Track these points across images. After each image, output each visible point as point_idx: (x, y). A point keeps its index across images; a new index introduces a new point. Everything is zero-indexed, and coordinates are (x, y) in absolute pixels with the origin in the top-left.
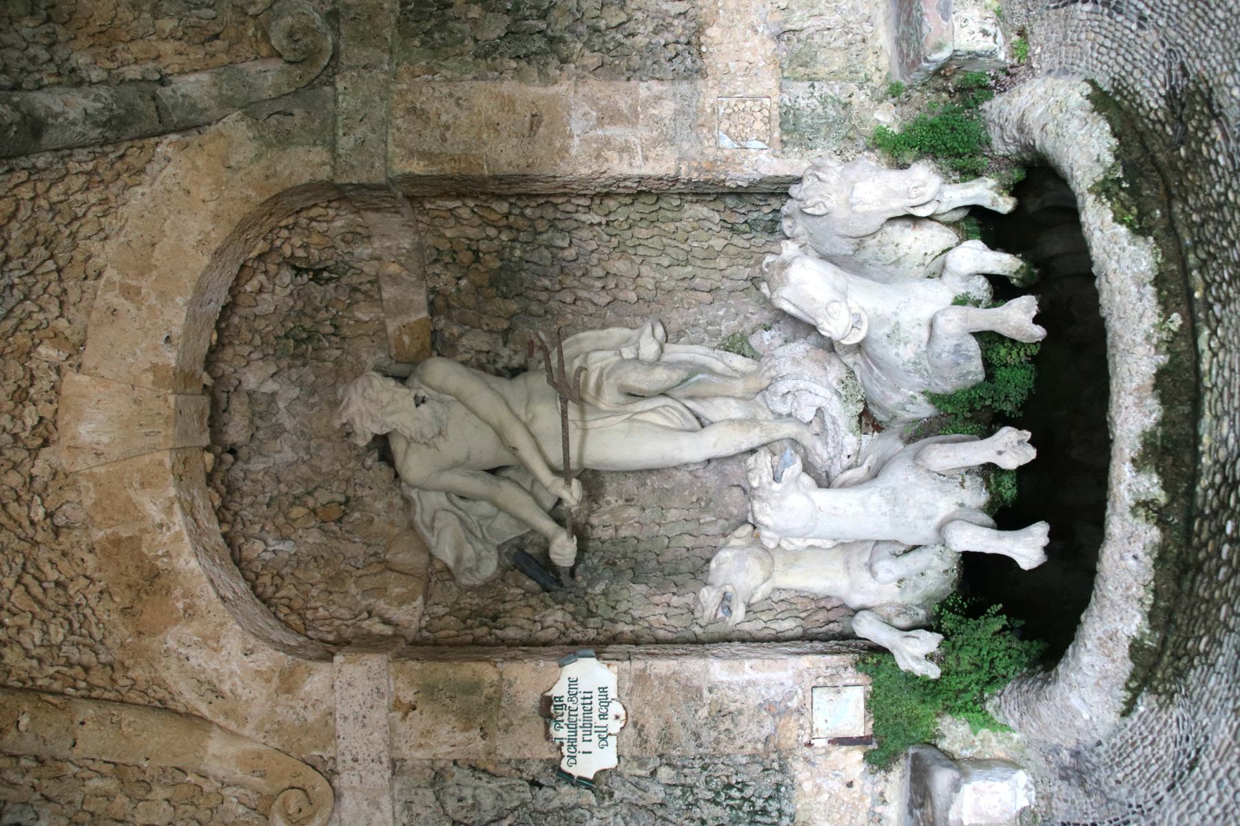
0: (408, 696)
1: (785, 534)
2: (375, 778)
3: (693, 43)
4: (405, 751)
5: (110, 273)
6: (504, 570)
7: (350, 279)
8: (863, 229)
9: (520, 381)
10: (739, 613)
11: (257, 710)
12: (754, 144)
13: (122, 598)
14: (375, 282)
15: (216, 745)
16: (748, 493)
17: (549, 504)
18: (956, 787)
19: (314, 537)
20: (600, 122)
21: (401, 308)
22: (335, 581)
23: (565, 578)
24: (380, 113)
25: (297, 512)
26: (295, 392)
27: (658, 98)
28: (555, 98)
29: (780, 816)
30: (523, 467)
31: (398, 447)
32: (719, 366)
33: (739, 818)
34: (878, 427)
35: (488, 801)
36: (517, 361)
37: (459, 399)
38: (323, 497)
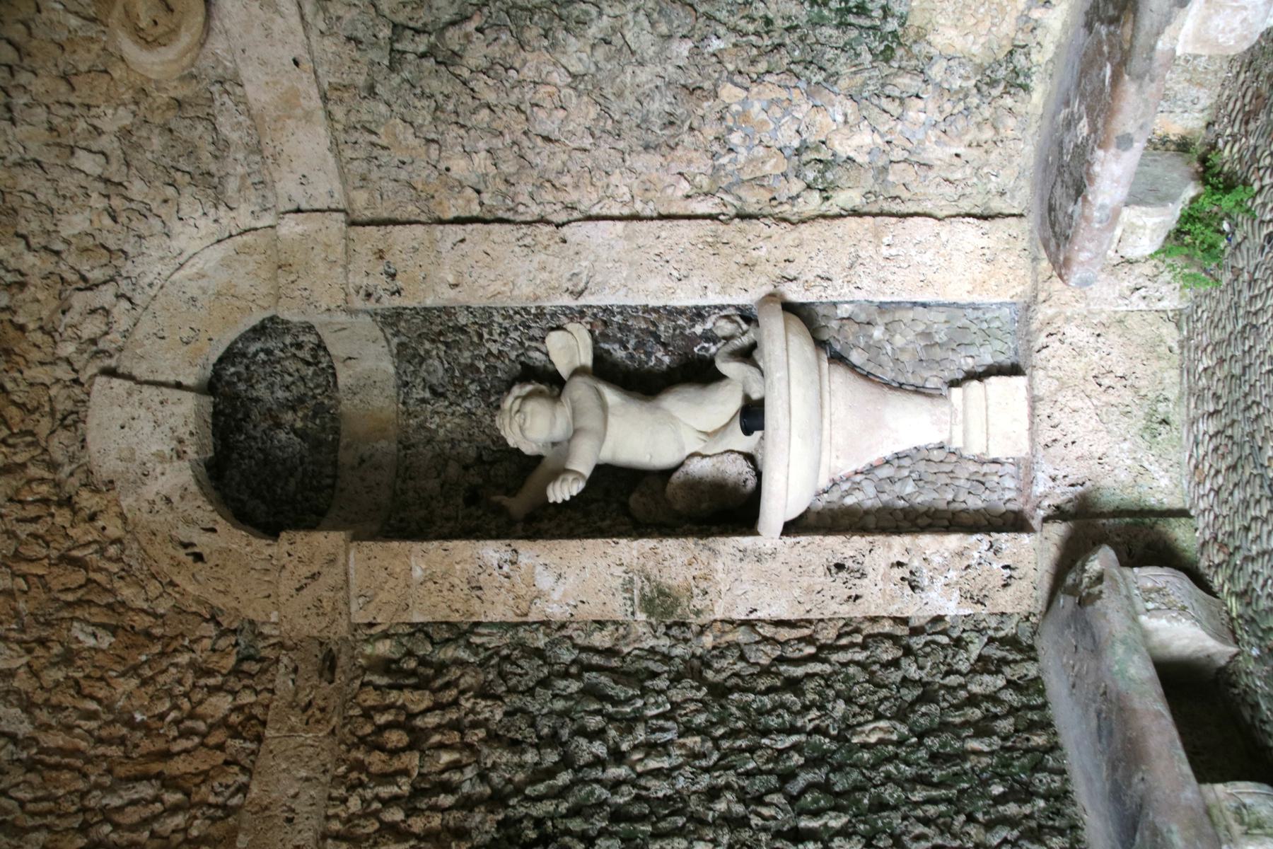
29: (885, 17)
33: (823, 18)
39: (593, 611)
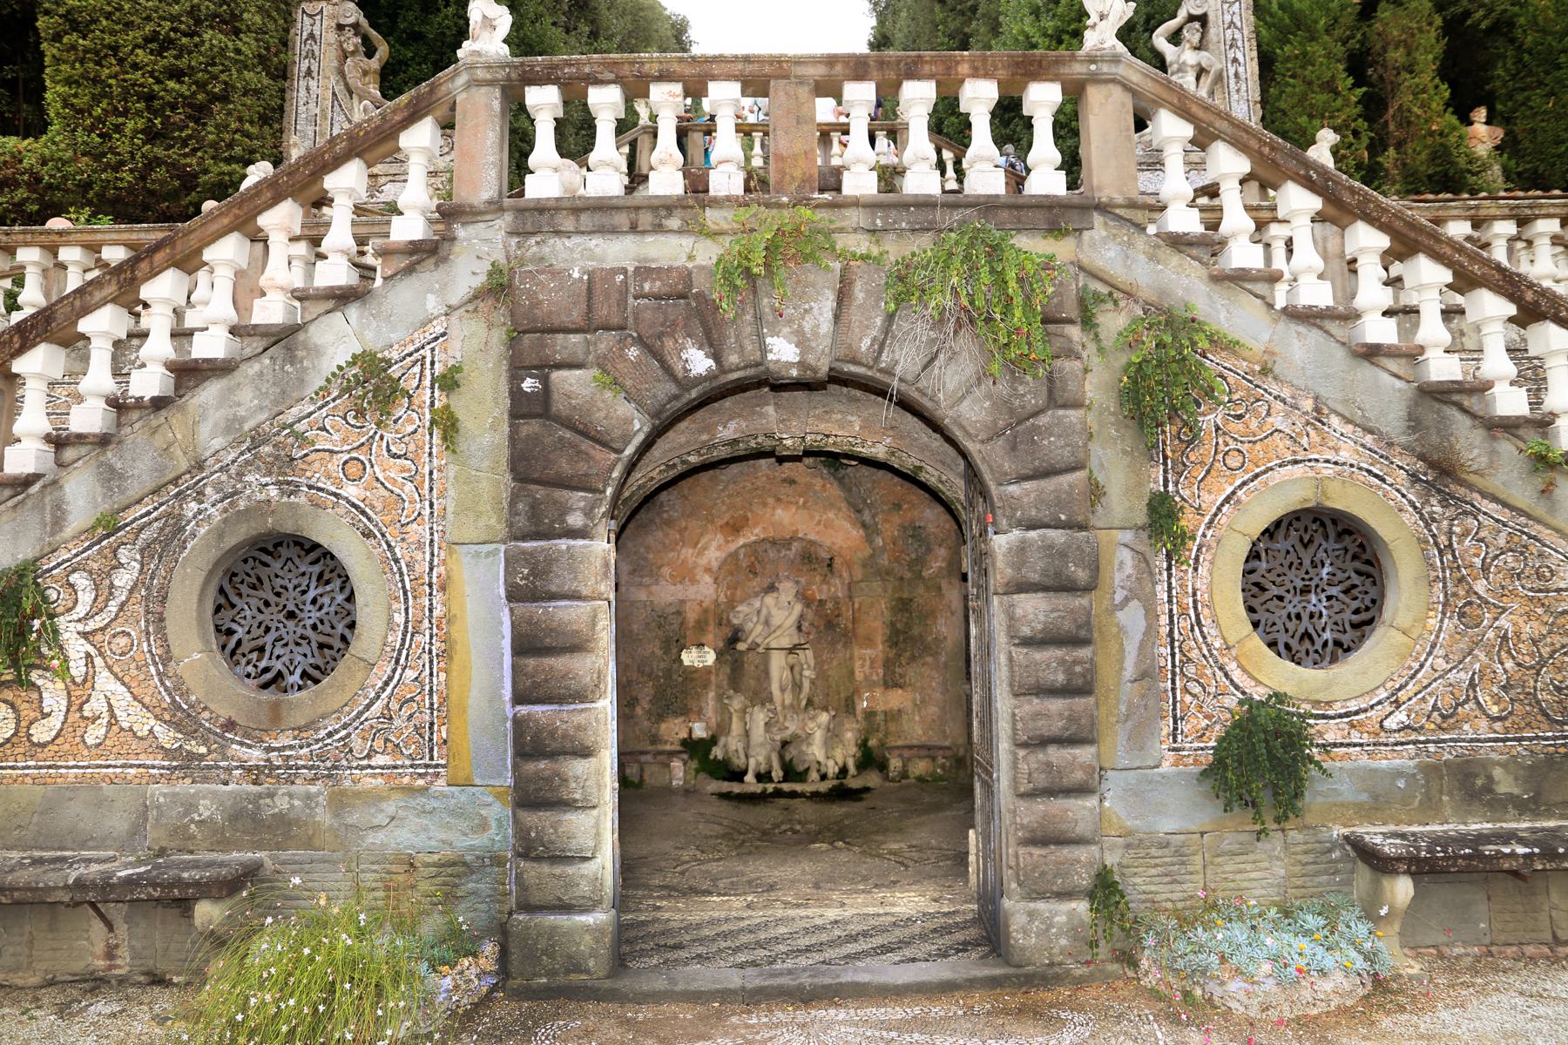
0: (704, 605)
1: (751, 715)
3: (897, 685)
10: (726, 701)
13: (731, 522)
14: (828, 583)
15: (691, 551)
16: (763, 705)
19: (744, 565)
21: (820, 591)
31: (775, 595)
34: (783, 747)
36: (803, 628)
38: (758, 566)
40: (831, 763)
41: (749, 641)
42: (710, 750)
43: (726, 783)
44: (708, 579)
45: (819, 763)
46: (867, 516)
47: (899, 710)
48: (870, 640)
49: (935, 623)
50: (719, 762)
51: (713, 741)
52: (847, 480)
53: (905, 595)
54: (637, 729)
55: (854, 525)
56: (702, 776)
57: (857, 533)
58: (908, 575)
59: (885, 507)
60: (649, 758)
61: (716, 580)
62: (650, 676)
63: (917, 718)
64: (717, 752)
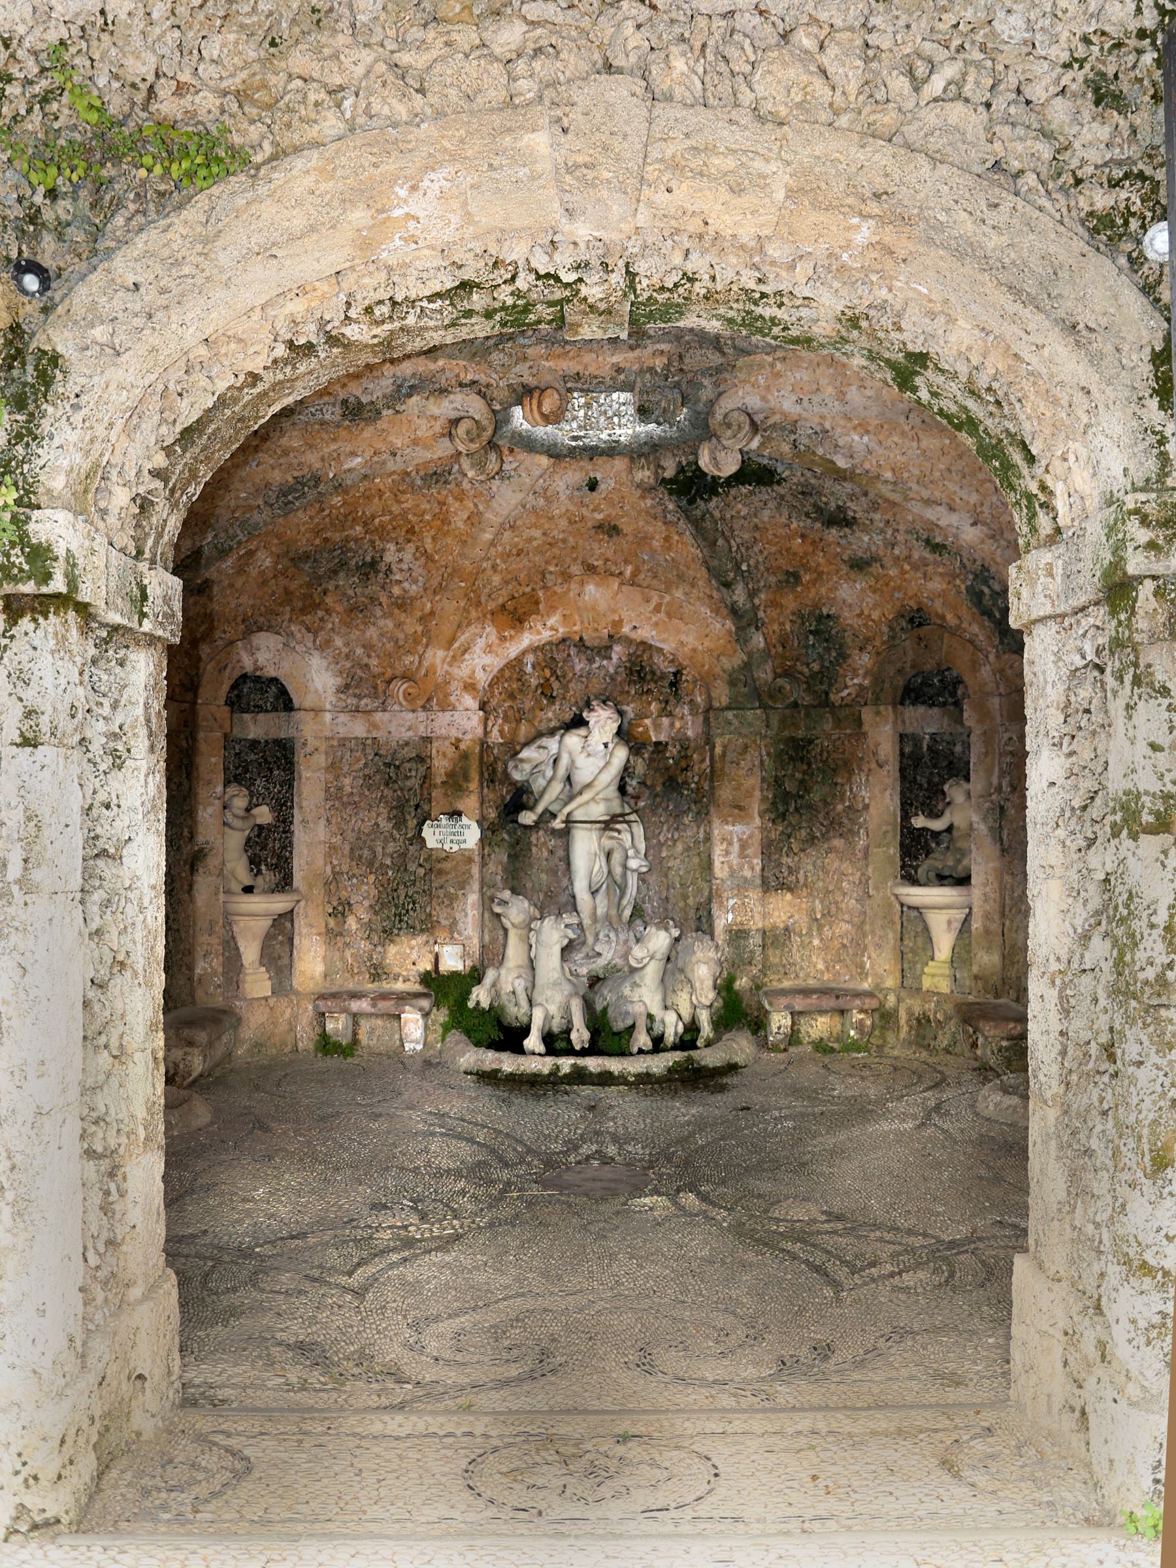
0: (463, 746)
1: (538, 932)
2: (422, 728)
3: (783, 886)
4: (435, 744)
5: (667, 598)
6: (514, 783)
7: (672, 701)
8: (687, 970)
9: (617, 794)
10: (497, 910)
11: (455, 671)
12: (730, 916)
14: (670, 714)
15: (441, 653)
16: (560, 914)
17: (553, 808)
18: (421, 1009)
19: (534, 682)
20: (740, 840)
21: (657, 727)
22: (512, 696)
23: (510, 817)
24: (745, 731)
25: (547, 672)
26: (612, 670)
27: (753, 869)
28: (752, 818)
30: (571, 798)
31: (583, 731)
32: (625, 902)
34: (591, 986)
35: (408, 783)
36: (630, 790)
37: (607, 764)
38: (556, 685)
39: (201, 829)
40: (671, 1017)
41: (540, 809)
42: (469, 993)
43: (491, 1055)
44: (470, 702)
45: (650, 1017)
46: (739, 595)
47: (787, 929)
48: (740, 808)
49: (849, 780)
50: (483, 1012)
51: (475, 976)
52: (708, 524)
53: (801, 734)
54: (348, 954)
55: (717, 612)
56: (455, 1036)
57: (723, 626)
58: (807, 699)
59: (772, 579)
60: (363, 1005)
61: (483, 706)
62: (370, 864)
63: (816, 942)
64: (480, 996)
